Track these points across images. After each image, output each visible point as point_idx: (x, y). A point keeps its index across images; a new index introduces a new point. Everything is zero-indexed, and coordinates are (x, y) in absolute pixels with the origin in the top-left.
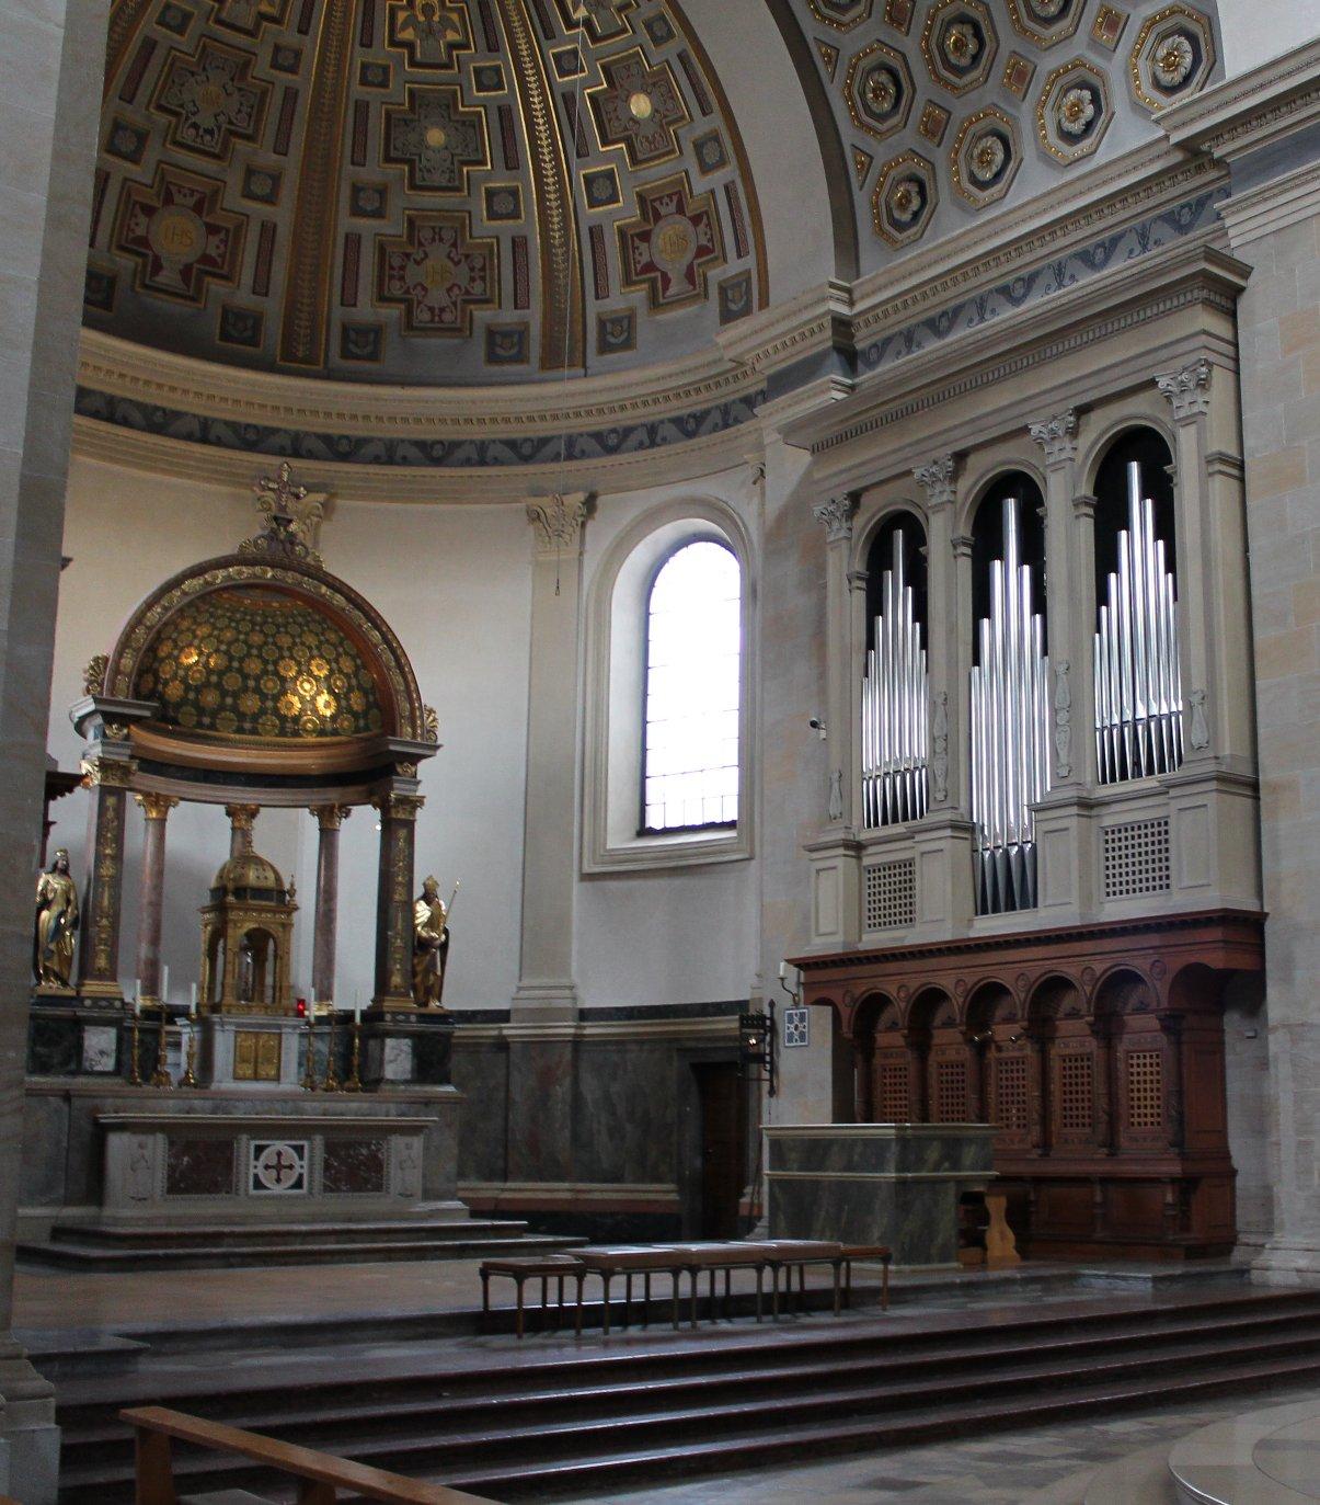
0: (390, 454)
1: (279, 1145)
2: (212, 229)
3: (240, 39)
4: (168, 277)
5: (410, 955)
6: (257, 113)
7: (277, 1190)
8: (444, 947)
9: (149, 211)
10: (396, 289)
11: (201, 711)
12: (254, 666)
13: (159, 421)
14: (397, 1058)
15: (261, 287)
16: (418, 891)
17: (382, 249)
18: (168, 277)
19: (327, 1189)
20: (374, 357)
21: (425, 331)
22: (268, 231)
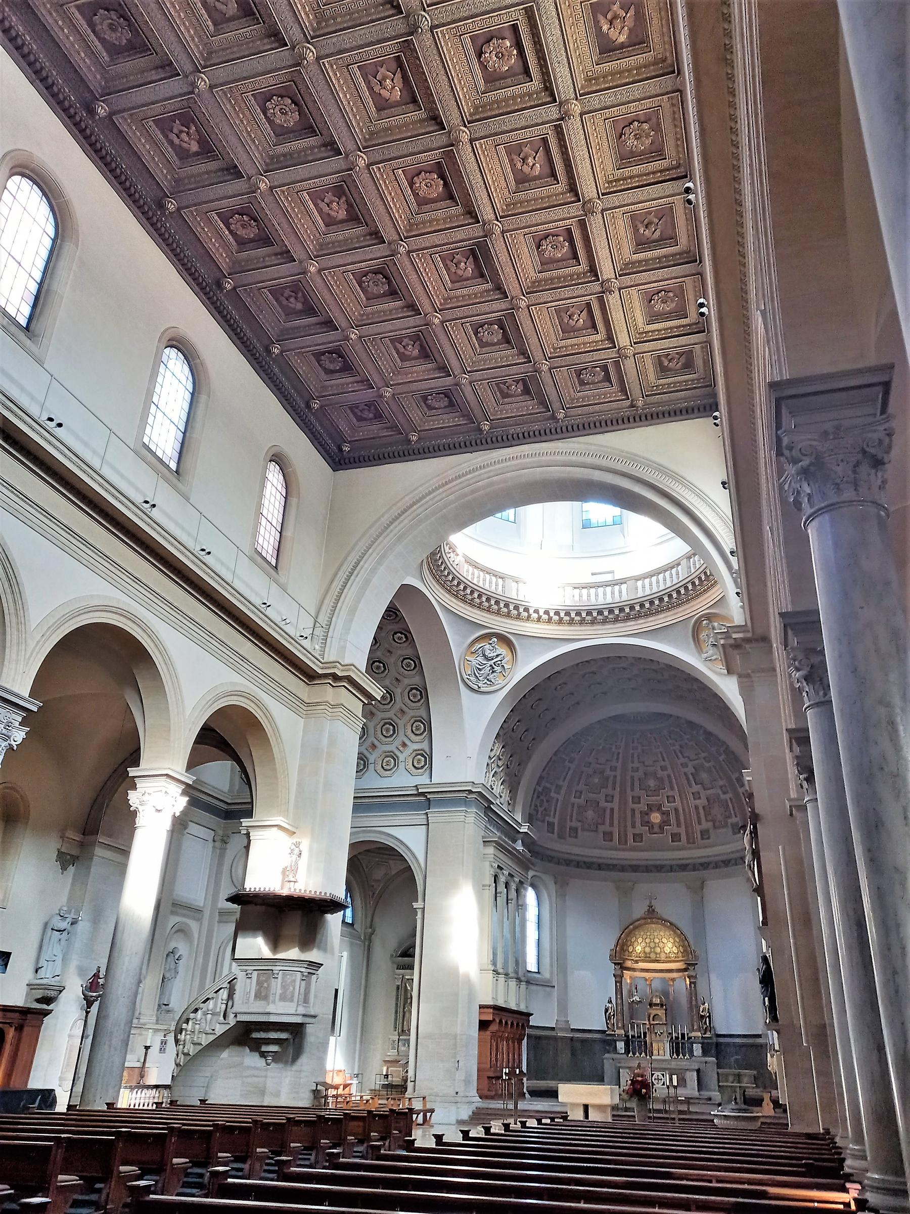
0: (716, 866)
1: (659, 1073)
2: (664, 814)
3: (652, 769)
4: (656, 829)
5: (704, 1019)
6: (663, 784)
7: (660, 1085)
8: (709, 1017)
9: (647, 814)
10: (710, 818)
11: (656, 954)
12: (657, 941)
13: (659, 868)
14: (697, 1049)
15: (679, 825)
16: (700, 1002)
17: (703, 807)
18: (656, 829)
19: (685, 1086)
20: (708, 838)
21: (719, 828)
22: (676, 810)
